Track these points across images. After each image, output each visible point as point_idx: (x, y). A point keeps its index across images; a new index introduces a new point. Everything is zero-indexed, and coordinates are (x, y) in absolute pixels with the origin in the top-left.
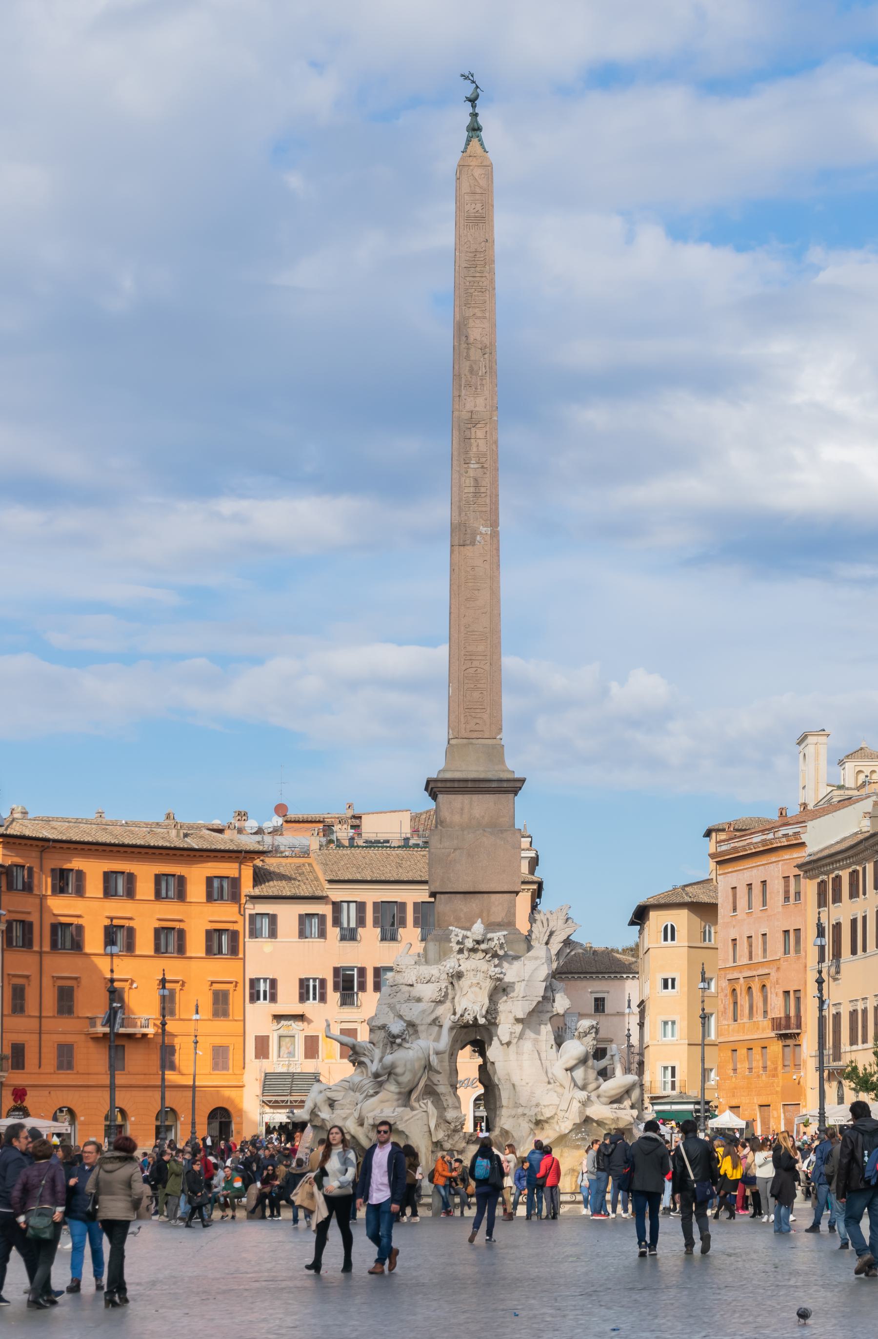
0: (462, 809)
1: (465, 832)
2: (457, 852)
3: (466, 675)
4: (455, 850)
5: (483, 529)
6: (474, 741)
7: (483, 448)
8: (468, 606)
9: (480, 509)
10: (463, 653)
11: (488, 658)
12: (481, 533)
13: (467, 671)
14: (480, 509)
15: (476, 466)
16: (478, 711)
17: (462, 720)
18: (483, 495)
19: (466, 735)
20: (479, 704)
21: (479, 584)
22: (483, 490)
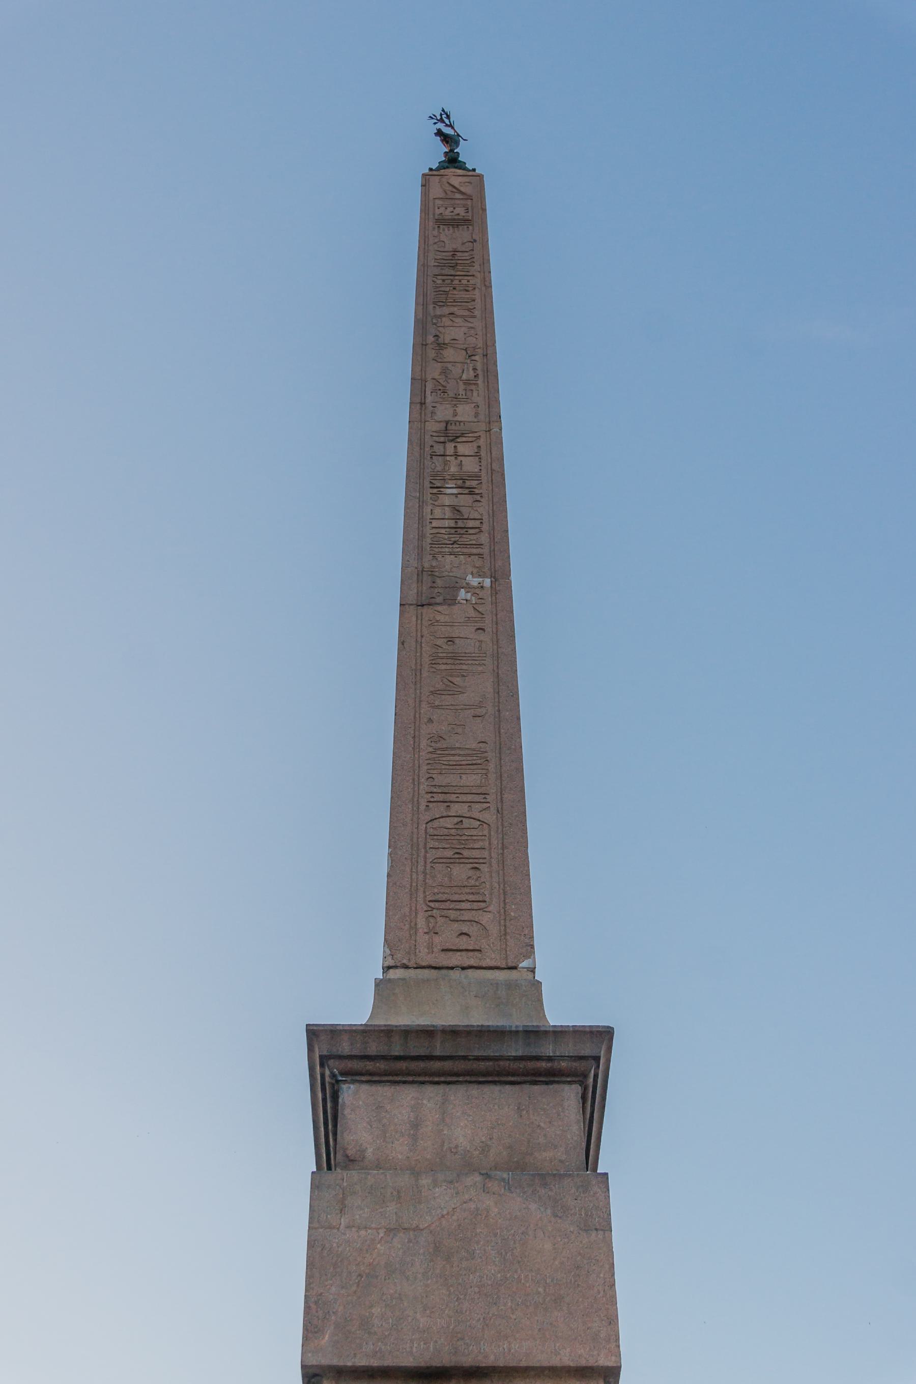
0: (416, 1125)
1: (425, 1181)
3: (431, 831)
5: (474, 581)
6: (455, 974)
7: (470, 465)
8: (437, 703)
9: (465, 550)
10: (424, 787)
11: (489, 798)
12: (468, 587)
13: (436, 824)
14: (465, 550)
15: (455, 491)
16: (463, 905)
17: (421, 922)
18: (471, 531)
20: (468, 890)
21: (464, 667)
22: (471, 524)
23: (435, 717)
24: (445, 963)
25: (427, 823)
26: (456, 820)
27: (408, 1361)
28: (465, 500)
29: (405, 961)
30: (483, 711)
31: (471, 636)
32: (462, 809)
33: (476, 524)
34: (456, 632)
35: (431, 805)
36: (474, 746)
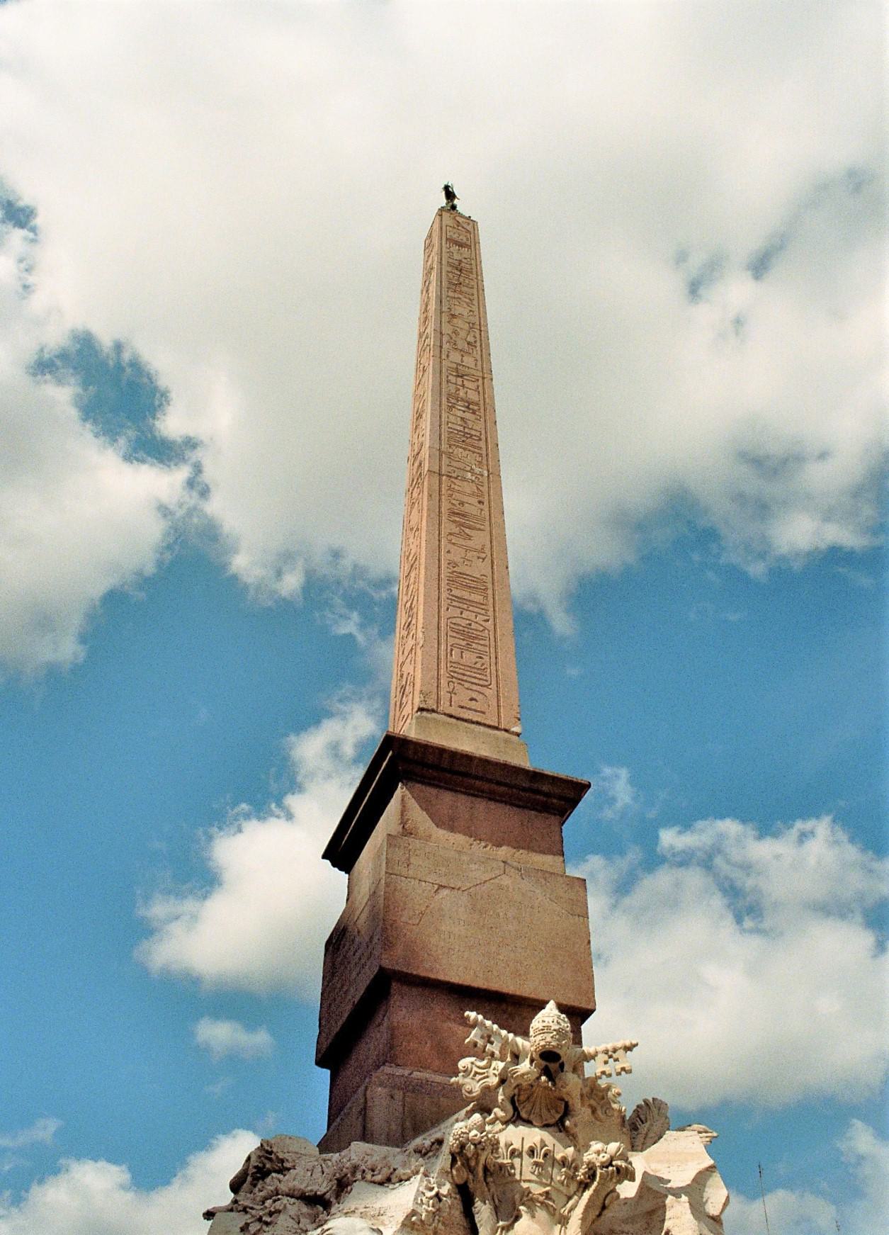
2: (445, 892)
4: (441, 887)
5: (477, 470)
8: (453, 541)
19: (454, 710)
21: (471, 523)
23: (452, 550)
24: (462, 715)
25: (448, 619)
26: (468, 622)
27: (455, 979)
28: (468, 415)
29: (435, 707)
30: (484, 555)
31: (475, 504)
32: (472, 616)
33: (478, 434)
34: (465, 499)
35: (450, 607)
36: (478, 576)
